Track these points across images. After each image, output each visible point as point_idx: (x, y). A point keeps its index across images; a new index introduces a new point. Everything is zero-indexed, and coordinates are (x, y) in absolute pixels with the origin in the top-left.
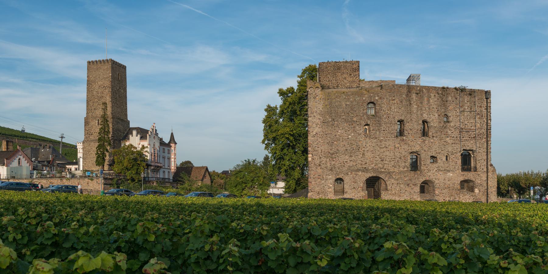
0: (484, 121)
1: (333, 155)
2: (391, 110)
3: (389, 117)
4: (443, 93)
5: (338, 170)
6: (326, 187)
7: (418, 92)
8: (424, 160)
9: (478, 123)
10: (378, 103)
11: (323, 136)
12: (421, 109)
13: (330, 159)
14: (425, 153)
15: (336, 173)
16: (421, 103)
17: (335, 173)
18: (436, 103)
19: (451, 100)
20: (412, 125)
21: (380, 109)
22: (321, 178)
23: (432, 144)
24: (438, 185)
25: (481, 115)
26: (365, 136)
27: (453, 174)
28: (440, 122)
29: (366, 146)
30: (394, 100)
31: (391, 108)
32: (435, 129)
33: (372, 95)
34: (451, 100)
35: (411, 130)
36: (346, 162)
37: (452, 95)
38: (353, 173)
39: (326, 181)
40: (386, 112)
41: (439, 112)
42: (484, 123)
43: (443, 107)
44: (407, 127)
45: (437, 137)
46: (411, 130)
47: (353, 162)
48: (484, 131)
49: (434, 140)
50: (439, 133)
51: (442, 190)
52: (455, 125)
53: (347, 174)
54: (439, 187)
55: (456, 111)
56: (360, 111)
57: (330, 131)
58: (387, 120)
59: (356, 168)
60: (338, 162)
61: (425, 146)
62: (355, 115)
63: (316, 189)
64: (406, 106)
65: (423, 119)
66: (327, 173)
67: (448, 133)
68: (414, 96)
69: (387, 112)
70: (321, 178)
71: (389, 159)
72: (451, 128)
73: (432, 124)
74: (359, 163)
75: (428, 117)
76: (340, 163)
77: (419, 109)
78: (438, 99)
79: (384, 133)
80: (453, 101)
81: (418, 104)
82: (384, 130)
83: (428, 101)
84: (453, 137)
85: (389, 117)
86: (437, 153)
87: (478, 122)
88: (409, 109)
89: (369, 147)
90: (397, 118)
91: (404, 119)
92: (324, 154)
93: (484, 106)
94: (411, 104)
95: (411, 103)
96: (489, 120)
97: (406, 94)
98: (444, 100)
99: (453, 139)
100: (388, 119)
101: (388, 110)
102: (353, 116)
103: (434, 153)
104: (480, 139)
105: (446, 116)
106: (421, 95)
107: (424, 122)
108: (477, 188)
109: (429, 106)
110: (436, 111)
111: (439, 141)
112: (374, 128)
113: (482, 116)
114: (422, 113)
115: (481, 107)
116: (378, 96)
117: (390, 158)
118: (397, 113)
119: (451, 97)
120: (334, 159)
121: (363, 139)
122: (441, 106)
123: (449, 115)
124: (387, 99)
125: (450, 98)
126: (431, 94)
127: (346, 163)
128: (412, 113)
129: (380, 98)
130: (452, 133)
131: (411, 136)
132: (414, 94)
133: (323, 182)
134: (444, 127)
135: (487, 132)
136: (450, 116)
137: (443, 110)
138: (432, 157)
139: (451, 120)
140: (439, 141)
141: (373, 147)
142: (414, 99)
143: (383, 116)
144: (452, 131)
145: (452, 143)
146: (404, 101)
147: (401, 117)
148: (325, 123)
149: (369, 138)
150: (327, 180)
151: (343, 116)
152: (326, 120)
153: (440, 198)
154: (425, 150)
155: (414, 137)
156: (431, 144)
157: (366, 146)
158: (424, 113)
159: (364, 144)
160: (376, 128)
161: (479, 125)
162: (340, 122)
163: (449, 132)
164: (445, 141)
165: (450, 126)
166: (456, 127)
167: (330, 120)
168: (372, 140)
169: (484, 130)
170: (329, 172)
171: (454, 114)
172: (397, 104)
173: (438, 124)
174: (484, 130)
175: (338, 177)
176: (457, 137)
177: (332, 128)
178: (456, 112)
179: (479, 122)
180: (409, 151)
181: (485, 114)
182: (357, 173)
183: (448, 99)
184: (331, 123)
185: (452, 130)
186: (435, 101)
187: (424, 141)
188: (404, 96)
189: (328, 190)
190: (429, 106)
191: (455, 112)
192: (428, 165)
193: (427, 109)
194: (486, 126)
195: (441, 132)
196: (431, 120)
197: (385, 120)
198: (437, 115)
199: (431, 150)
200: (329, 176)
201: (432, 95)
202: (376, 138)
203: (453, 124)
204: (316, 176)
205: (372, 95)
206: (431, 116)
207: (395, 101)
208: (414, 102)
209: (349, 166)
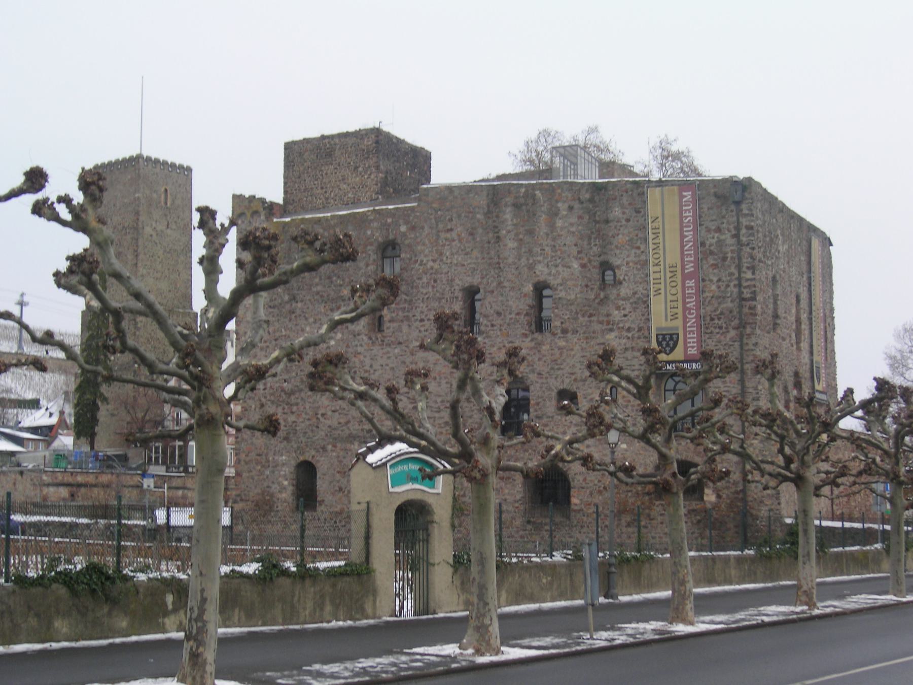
0: (731, 274)
1: (293, 397)
2: (442, 260)
3: (435, 281)
4: (597, 198)
5: (304, 440)
6: (274, 486)
7: (522, 200)
8: (538, 404)
9: (711, 281)
10: (407, 242)
11: (268, 344)
12: (530, 251)
13: (284, 409)
14: (540, 381)
15: (298, 448)
16: (531, 232)
17: (295, 446)
18: (573, 229)
19: (621, 216)
20: (500, 298)
21: (410, 259)
22: (263, 461)
23: (561, 354)
24: (581, 478)
25: (721, 255)
26: (370, 338)
27: (627, 444)
28: (587, 286)
29: (371, 366)
30: (451, 230)
31: (441, 254)
32: (573, 308)
33: (389, 220)
34: (621, 216)
35: (499, 314)
36: (323, 415)
37: (625, 200)
38: (339, 445)
39: (273, 472)
40: (429, 266)
41: (583, 255)
42: (730, 281)
43: (595, 238)
44: (488, 305)
45: (575, 332)
46: (499, 314)
47: (340, 414)
48: (730, 305)
49: (567, 341)
50: (582, 320)
51: (591, 494)
52: (635, 293)
53: (324, 448)
54: (584, 485)
55: (638, 248)
56: (360, 269)
57: (285, 330)
58: (430, 289)
59: (347, 432)
60: (304, 415)
61: (540, 359)
62: (347, 280)
63: (251, 494)
64: (486, 245)
65: (536, 279)
66: (277, 449)
67: (611, 318)
68: (508, 215)
69: (432, 268)
70: (263, 461)
71: (436, 402)
72: (621, 302)
73: (562, 294)
74: (354, 418)
75: (550, 274)
76: (309, 419)
77: (523, 250)
78: (580, 217)
79: (422, 329)
80: (628, 220)
81: (521, 236)
82: (422, 320)
83: (552, 226)
84: (629, 330)
85: (435, 281)
86: (575, 380)
87: (712, 277)
88: (493, 253)
89: (380, 372)
90: (460, 283)
91: (480, 283)
92: (272, 394)
93: (731, 227)
94: (498, 237)
95: (500, 234)
96: (748, 268)
97: (486, 211)
98: (597, 218)
99: (630, 335)
100: (433, 287)
101: (434, 261)
102: (341, 286)
103: (567, 381)
104: (717, 330)
105: (606, 266)
106: (528, 211)
107: (540, 289)
108: (709, 487)
109: (554, 239)
110: (575, 253)
111: (584, 345)
112: (394, 315)
113: (724, 259)
114: (531, 261)
115: (718, 230)
116: (407, 222)
117: (439, 400)
118: (459, 269)
119: (622, 206)
120: (295, 409)
121: (365, 347)
122: (590, 238)
123: (616, 261)
124: (431, 228)
125: (617, 212)
126: (560, 205)
127: (322, 419)
128: (502, 265)
129: (413, 228)
130: (625, 316)
131: (499, 333)
132: (509, 209)
133: (267, 472)
134: (597, 301)
135: (741, 307)
136: (618, 267)
137: (595, 249)
138: (563, 394)
139: (621, 278)
140: (584, 345)
141: (392, 369)
142: (510, 223)
143: (420, 279)
144: (623, 312)
145: (626, 349)
146: (480, 231)
147: (469, 279)
148: (274, 307)
149: (380, 345)
150: (276, 466)
151: (317, 285)
152: (275, 299)
153: (585, 519)
154: (539, 374)
155: (508, 335)
156: (557, 352)
157: (371, 366)
158: (540, 262)
159: (368, 361)
160: (400, 313)
161: (714, 287)
162: (308, 302)
163: (616, 315)
164: (602, 341)
165: (618, 295)
166: (639, 299)
167: (286, 298)
168: (388, 349)
169: (732, 301)
170: (282, 446)
171: (632, 258)
172: (460, 241)
173: (581, 292)
174: (732, 301)
175: (302, 458)
176: (640, 329)
177: (290, 320)
178: (638, 252)
179: (715, 279)
180: (492, 378)
181: (732, 251)
182: (348, 445)
183: (611, 216)
184: (288, 307)
185: (624, 309)
186: (572, 225)
187: (540, 344)
188: (478, 216)
189: (279, 496)
190: (554, 239)
191: (633, 251)
192: (549, 417)
193: (547, 249)
194: (736, 290)
195: (591, 315)
196: (559, 281)
197: (425, 291)
198: (575, 265)
199: (560, 372)
200: (282, 455)
201: (562, 206)
202: (400, 343)
203: (628, 291)
204: (253, 455)
205: (389, 220)
206: (560, 269)
207: (454, 235)
208: (509, 232)
209: (330, 427)
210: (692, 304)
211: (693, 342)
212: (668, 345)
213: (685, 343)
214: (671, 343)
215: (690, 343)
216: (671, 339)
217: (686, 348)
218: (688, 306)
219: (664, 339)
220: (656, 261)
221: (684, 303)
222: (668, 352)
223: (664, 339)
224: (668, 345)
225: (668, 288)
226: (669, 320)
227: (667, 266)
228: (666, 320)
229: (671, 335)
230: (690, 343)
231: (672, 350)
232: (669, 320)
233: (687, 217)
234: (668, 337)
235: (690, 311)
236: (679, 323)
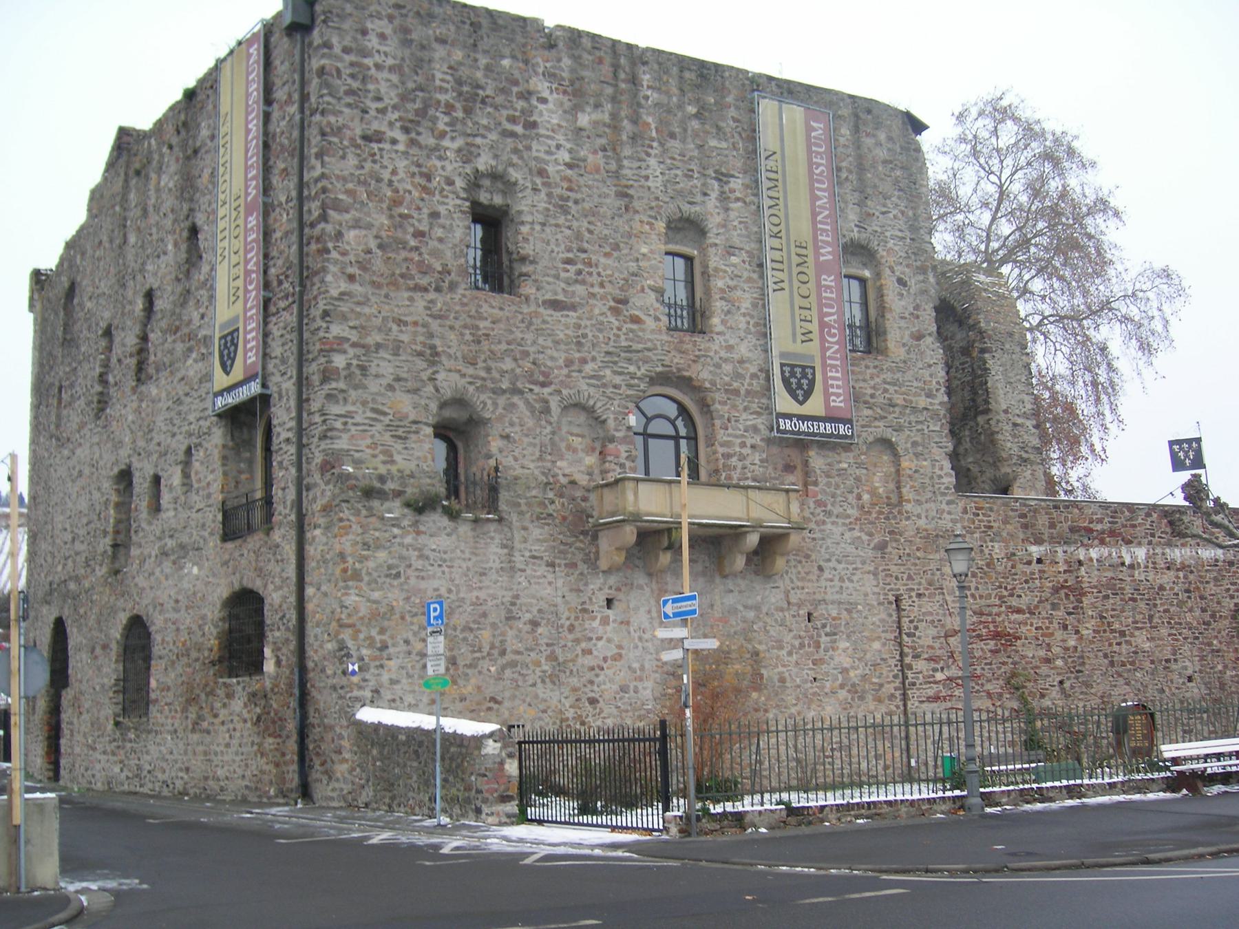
213: (826, 387)
214: (805, 382)
216: (804, 376)
217: (827, 395)
218: (826, 319)
219: (793, 374)
220: (776, 230)
221: (822, 316)
222: (801, 398)
223: (793, 374)
224: (800, 386)
225: (796, 284)
227: (793, 246)
229: (804, 367)
230: (832, 386)
232: (799, 341)
234: (798, 370)
236: (814, 348)
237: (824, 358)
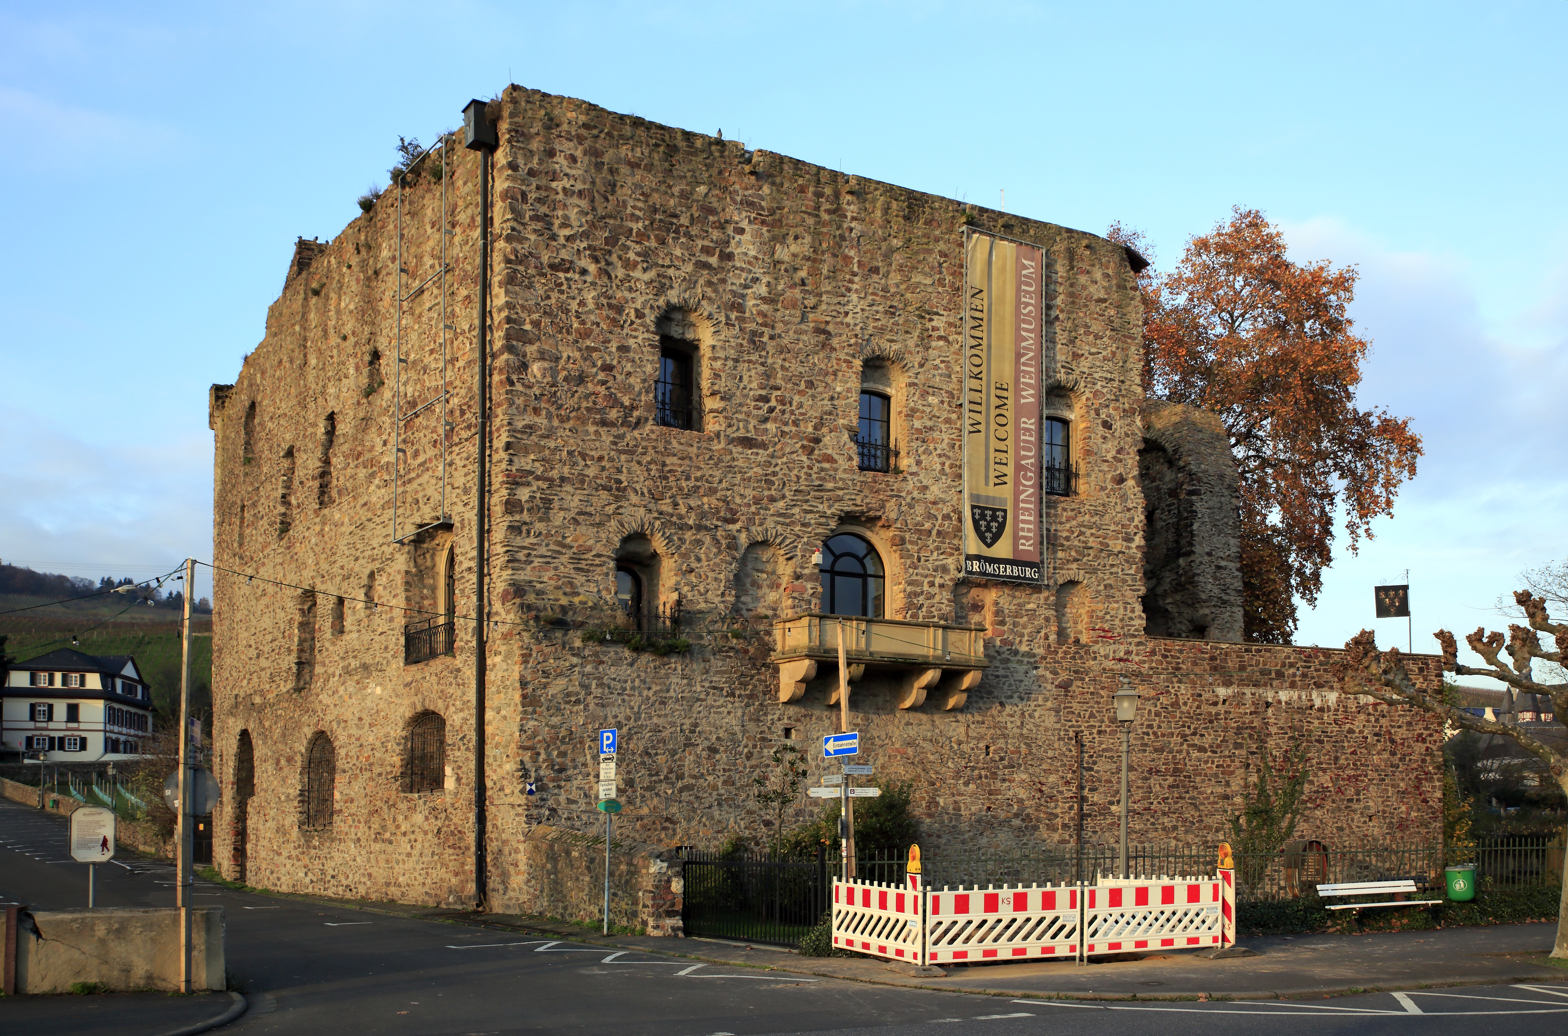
210: (1029, 461)
211: (1029, 530)
212: (989, 528)
214: (994, 525)
215: (1023, 530)
217: (1016, 538)
218: (1023, 462)
219: (983, 516)
220: (976, 370)
221: (1018, 459)
222: (989, 541)
223: (983, 516)
224: (989, 528)
225: (993, 426)
226: (991, 484)
228: (987, 484)
229: (994, 510)
231: (996, 537)
232: (991, 484)
233: (1027, 304)
235: (1026, 474)
237: (1016, 501)
